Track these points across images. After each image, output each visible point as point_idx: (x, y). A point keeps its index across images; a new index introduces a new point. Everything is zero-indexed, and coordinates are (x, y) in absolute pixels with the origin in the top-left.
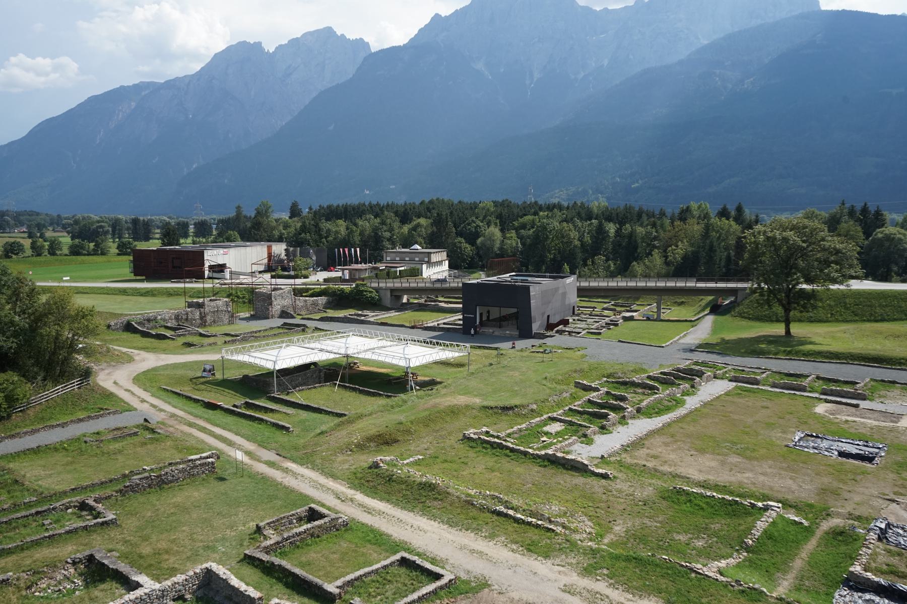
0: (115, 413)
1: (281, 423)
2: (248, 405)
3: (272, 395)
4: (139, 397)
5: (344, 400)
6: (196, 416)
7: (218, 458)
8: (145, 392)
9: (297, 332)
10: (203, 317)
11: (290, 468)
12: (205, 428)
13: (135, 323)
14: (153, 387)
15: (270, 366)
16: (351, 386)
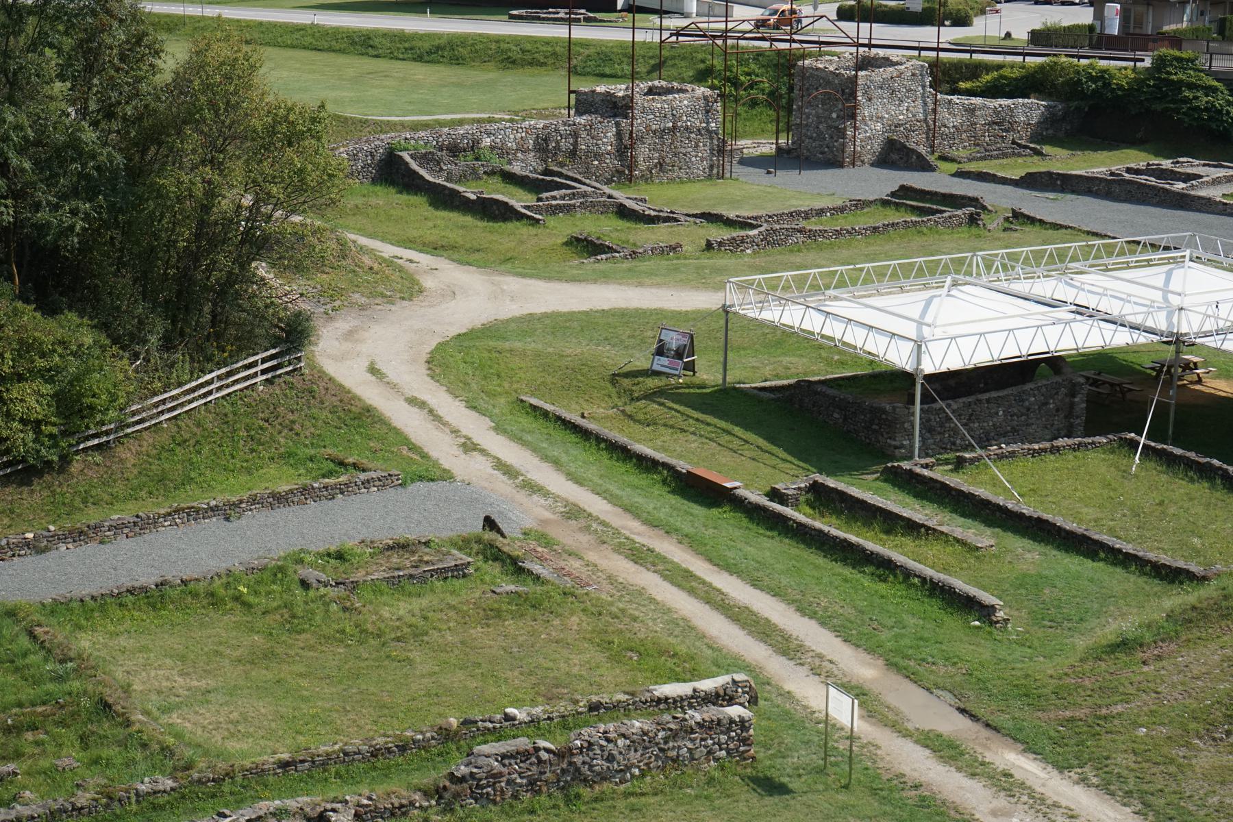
0: (384, 482)
1: (960, 584)
2: (821, 497)
3: (906, 465)
4: (455, 432)
5: (1172, 510)
6: (652, 523)
7: (753, 701)
8: (474, 414)
9: (950, 223)
10: (624, 149)
11: (1018, 775)
12: (688, 575)
13: (412, 156)
14: (492, 395)
15: (899, 357)
16: (1192, 455)
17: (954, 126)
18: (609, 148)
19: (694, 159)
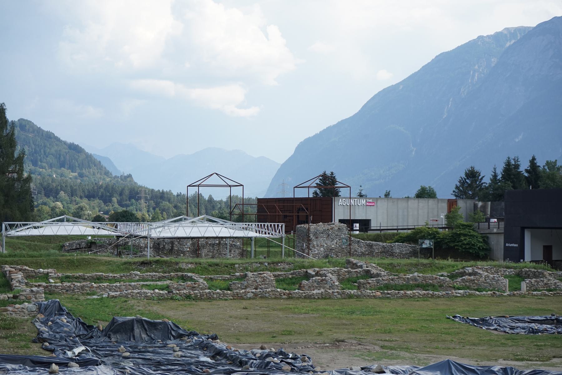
17: (361, 252)
18: (188, 249)
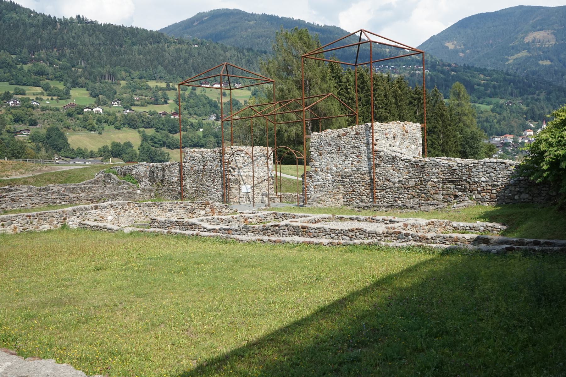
19: (213, 190)
